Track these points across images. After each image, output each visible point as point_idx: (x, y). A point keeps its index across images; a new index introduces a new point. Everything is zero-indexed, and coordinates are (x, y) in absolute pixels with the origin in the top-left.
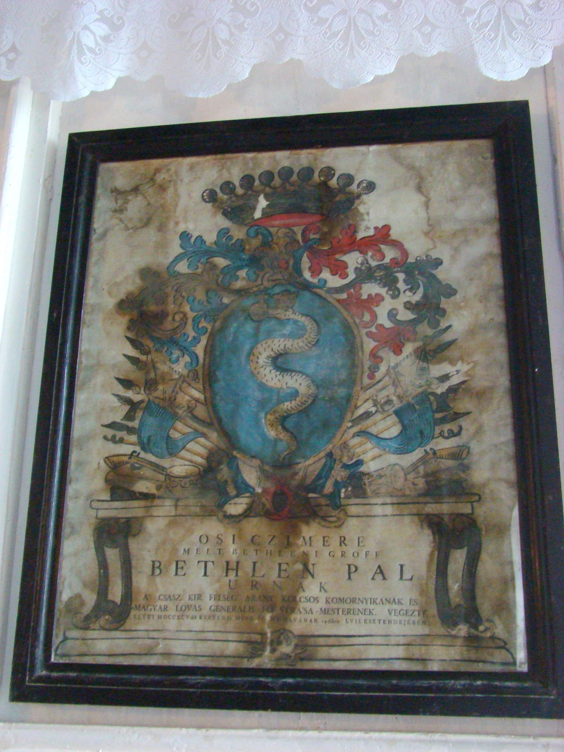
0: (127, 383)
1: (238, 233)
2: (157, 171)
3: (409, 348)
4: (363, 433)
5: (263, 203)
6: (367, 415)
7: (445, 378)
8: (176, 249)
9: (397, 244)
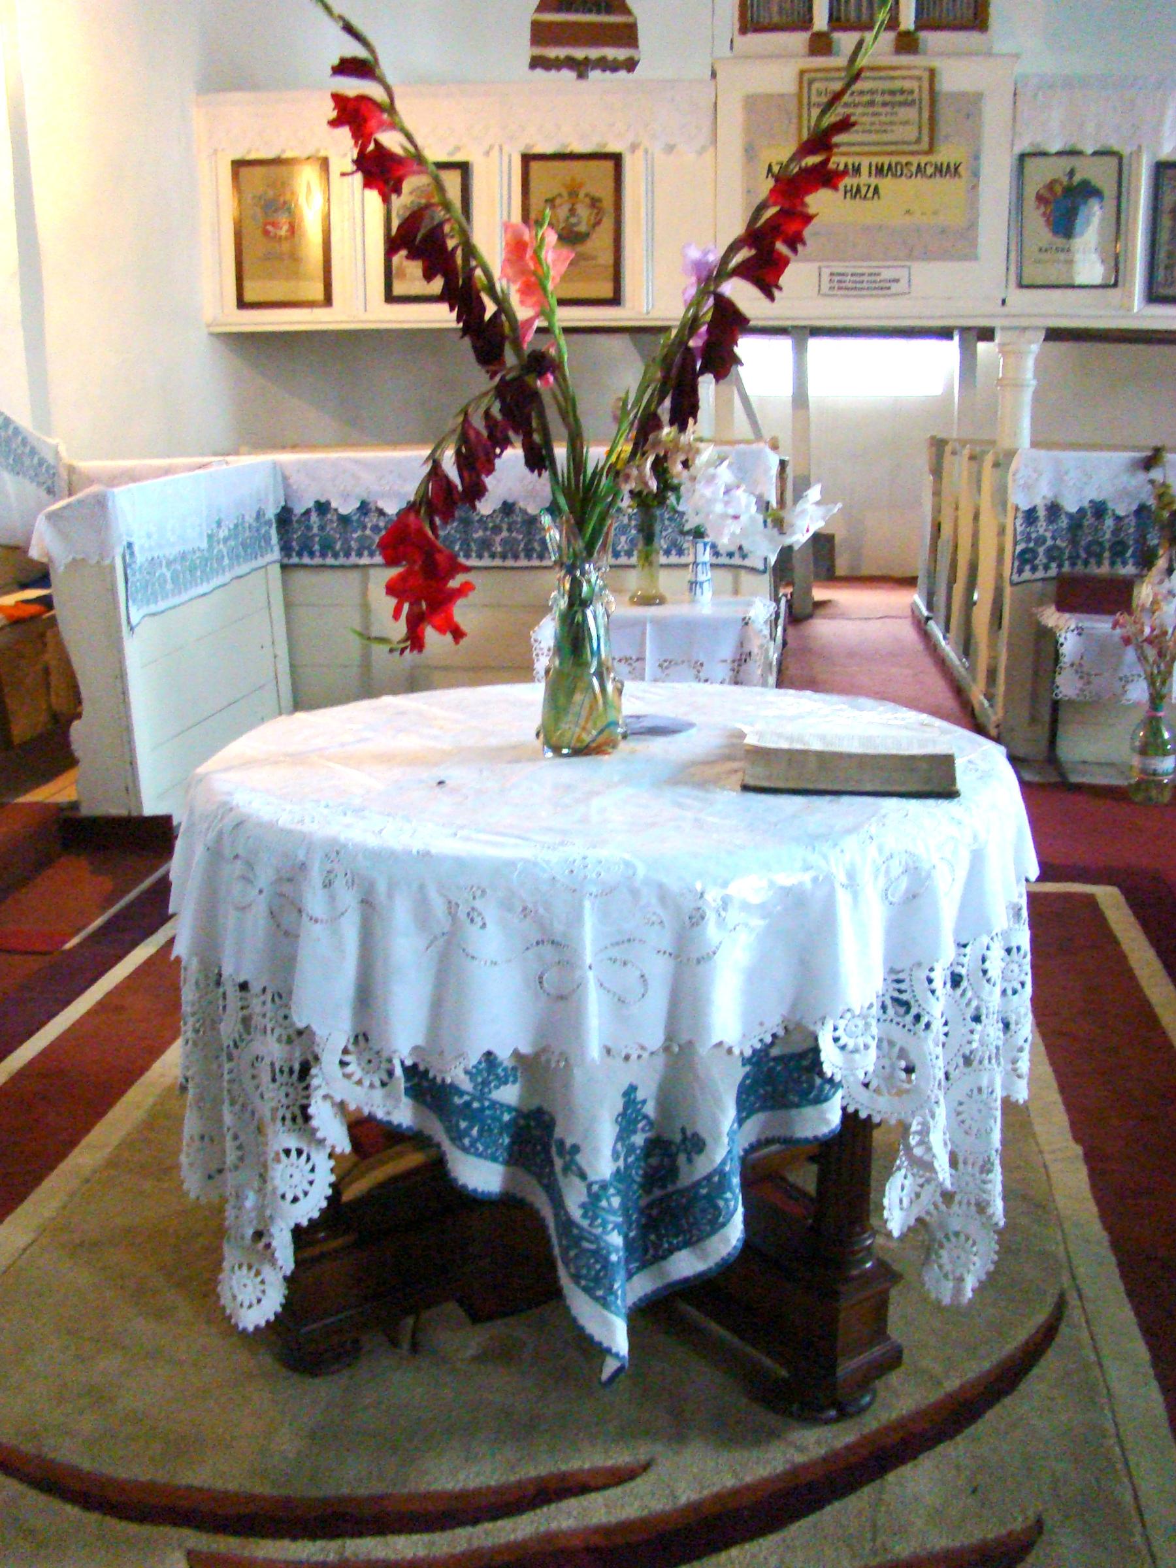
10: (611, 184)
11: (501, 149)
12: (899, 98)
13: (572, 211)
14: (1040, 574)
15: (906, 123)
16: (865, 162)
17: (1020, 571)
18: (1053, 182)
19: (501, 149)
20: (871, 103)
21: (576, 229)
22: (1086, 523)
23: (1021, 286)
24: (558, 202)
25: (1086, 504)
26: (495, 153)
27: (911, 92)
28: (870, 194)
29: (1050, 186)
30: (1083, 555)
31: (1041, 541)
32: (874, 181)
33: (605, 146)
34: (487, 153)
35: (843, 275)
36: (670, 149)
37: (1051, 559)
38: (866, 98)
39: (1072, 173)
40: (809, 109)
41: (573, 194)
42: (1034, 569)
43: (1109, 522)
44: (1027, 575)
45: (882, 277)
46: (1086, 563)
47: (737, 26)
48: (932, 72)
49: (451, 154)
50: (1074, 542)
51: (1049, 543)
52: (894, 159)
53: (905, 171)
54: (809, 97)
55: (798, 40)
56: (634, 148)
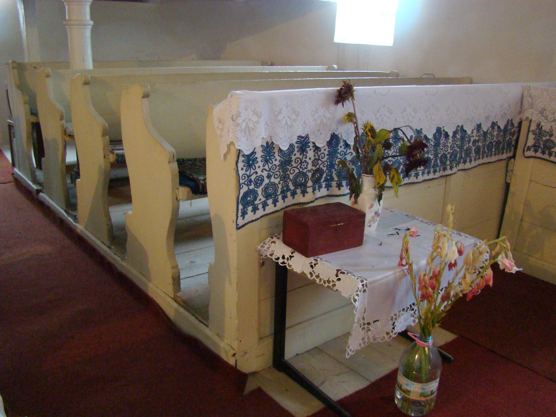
14: (260, 213)
17: (244, 214)
22: (294, 158)
25: (294, 140)
30: (292, 187)
31: (260, 181)
37: (268, 196)
42: (255, 209)
43: (311, 154)
44: (250, 216)
46: (294, 194)
50: (285, 178)
51: (266, 181)
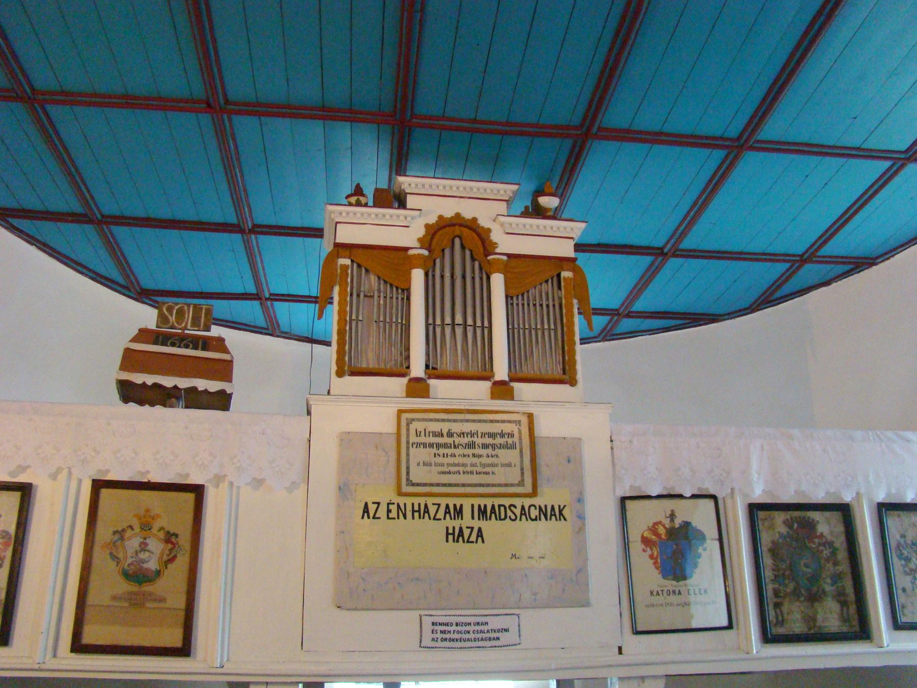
0: (774, 570)
1: (791, 533)
2: (770, 514)
3: (831, 563)
4: (825, 583)
5: (796, 525)
6: (824, 578)
7: (838, 570)
8: (777, 535)
9: (825, 537)
10: (190, 516)
11: (70, 473)
12: (499, 441)
13: (143, 547)
15: (509, 465)
16: (467, 503)
18: (656, 524)
19: (70, 473)
20: (471, 445)
21: (145, 565)
23: (637, 633)
24: (129, 533)
26: (63, 476)
27: (511, 435)
28: (473, 538)
29: (653, 529)
32: (476, 524)
33: (188, 475)
34: (54, 476)
35: (447, 624)
36: (258, 483)
38: (466, 440)
39: (672, 516)
40: (408, 448)
41: (146, 527)
45: (489, 627)
47: (334, 368)
48: (530, 416)
49: (11, 474)
52: (497, 501)
53: (509, 513)
54: (408, 435)
55: (398, 384)
56: (218, 479)
